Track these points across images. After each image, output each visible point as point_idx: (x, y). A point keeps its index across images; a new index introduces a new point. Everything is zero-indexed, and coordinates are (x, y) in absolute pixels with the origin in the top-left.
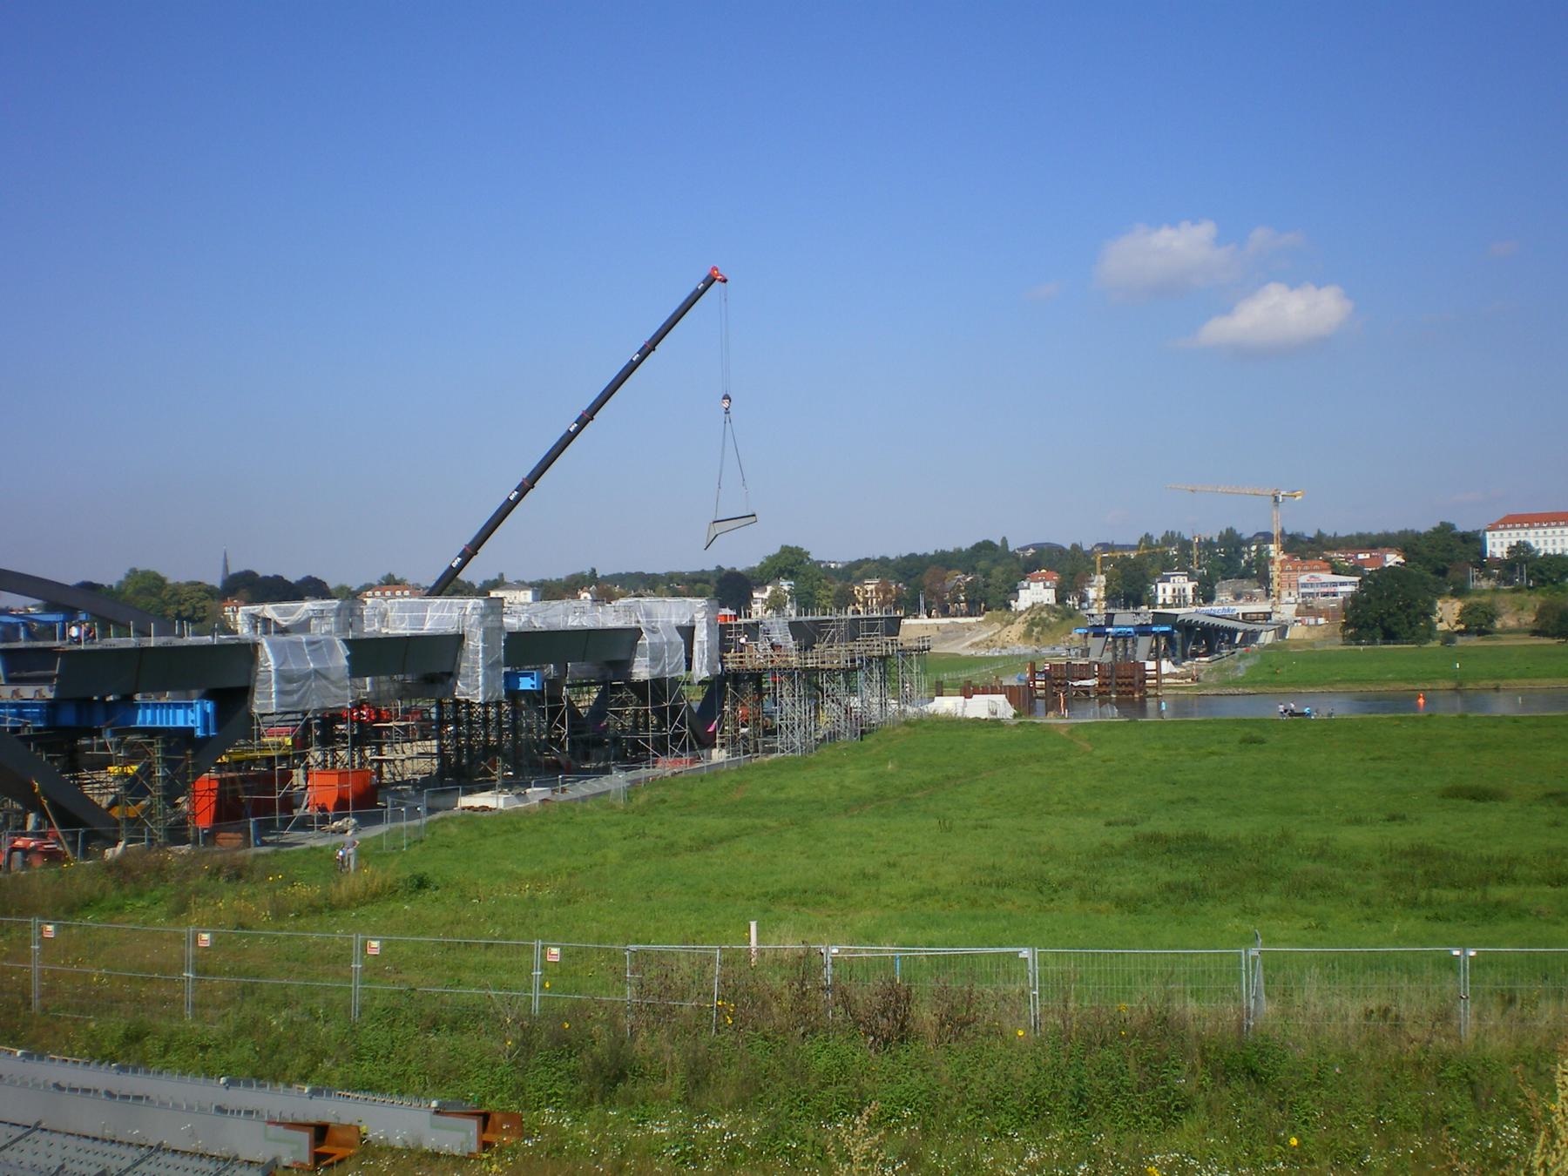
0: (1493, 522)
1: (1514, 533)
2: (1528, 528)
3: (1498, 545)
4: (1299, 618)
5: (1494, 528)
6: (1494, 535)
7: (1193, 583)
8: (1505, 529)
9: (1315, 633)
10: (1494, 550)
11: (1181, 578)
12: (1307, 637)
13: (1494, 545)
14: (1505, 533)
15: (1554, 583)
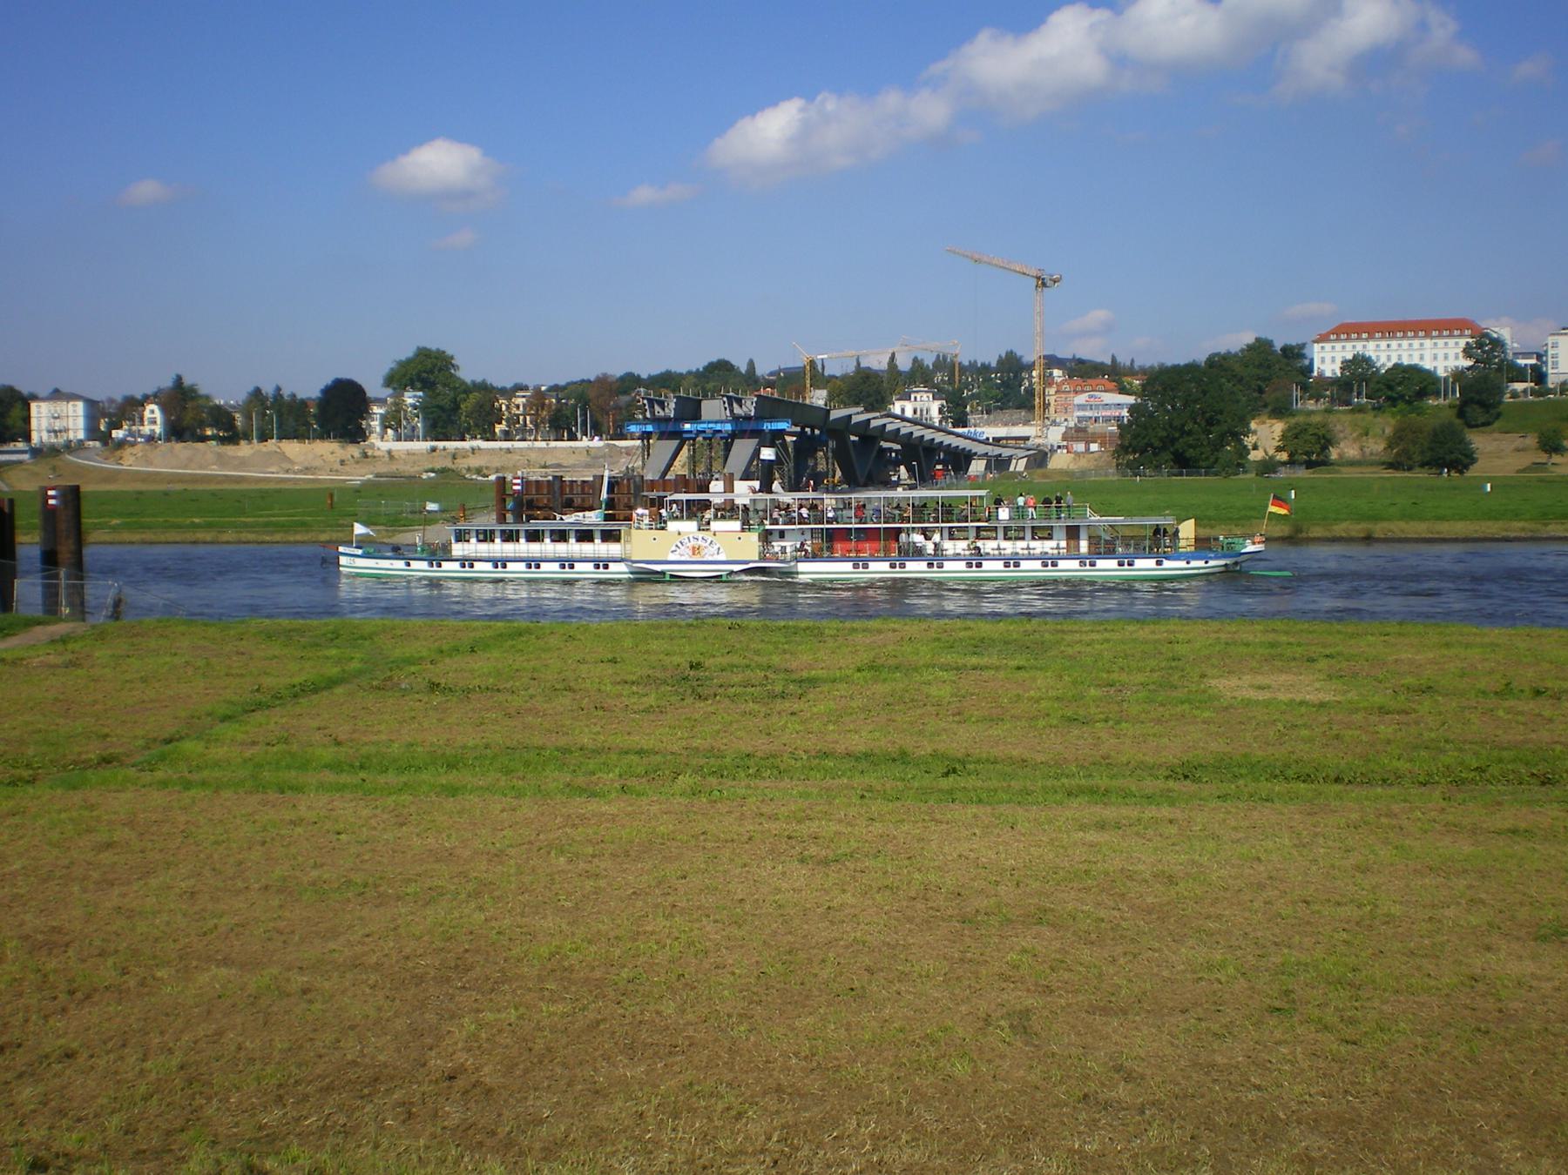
0: (1323, 332)
1: (1349, 345)
2: (1367, 340)
3: (1328, 360)
4: (1065, 443)
5: (1323, 338)
6: (1323, 348)
7: (939, 402)
8: (1338, 340)
9: (1083, 463)
10: (1322, 367)
11: (925, 396)
12: (1072, 466)
13: (1323, 360)
14: (1338, 346)
15: (1409, 403)
